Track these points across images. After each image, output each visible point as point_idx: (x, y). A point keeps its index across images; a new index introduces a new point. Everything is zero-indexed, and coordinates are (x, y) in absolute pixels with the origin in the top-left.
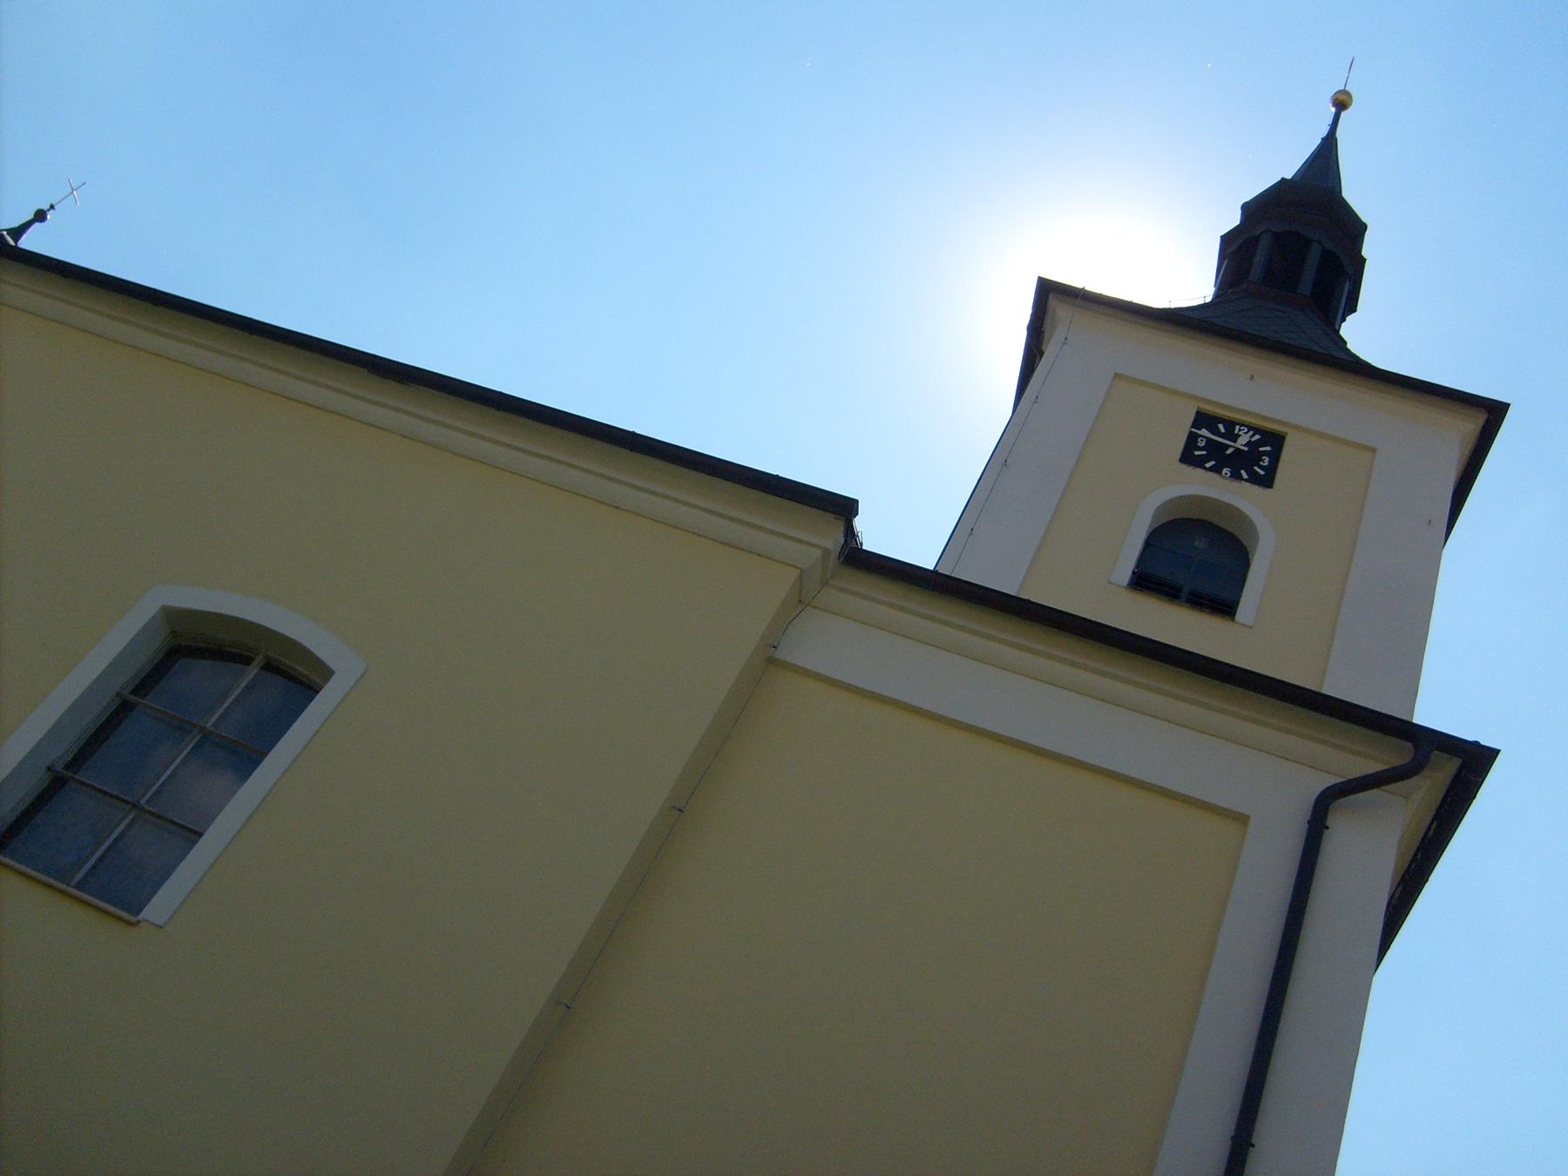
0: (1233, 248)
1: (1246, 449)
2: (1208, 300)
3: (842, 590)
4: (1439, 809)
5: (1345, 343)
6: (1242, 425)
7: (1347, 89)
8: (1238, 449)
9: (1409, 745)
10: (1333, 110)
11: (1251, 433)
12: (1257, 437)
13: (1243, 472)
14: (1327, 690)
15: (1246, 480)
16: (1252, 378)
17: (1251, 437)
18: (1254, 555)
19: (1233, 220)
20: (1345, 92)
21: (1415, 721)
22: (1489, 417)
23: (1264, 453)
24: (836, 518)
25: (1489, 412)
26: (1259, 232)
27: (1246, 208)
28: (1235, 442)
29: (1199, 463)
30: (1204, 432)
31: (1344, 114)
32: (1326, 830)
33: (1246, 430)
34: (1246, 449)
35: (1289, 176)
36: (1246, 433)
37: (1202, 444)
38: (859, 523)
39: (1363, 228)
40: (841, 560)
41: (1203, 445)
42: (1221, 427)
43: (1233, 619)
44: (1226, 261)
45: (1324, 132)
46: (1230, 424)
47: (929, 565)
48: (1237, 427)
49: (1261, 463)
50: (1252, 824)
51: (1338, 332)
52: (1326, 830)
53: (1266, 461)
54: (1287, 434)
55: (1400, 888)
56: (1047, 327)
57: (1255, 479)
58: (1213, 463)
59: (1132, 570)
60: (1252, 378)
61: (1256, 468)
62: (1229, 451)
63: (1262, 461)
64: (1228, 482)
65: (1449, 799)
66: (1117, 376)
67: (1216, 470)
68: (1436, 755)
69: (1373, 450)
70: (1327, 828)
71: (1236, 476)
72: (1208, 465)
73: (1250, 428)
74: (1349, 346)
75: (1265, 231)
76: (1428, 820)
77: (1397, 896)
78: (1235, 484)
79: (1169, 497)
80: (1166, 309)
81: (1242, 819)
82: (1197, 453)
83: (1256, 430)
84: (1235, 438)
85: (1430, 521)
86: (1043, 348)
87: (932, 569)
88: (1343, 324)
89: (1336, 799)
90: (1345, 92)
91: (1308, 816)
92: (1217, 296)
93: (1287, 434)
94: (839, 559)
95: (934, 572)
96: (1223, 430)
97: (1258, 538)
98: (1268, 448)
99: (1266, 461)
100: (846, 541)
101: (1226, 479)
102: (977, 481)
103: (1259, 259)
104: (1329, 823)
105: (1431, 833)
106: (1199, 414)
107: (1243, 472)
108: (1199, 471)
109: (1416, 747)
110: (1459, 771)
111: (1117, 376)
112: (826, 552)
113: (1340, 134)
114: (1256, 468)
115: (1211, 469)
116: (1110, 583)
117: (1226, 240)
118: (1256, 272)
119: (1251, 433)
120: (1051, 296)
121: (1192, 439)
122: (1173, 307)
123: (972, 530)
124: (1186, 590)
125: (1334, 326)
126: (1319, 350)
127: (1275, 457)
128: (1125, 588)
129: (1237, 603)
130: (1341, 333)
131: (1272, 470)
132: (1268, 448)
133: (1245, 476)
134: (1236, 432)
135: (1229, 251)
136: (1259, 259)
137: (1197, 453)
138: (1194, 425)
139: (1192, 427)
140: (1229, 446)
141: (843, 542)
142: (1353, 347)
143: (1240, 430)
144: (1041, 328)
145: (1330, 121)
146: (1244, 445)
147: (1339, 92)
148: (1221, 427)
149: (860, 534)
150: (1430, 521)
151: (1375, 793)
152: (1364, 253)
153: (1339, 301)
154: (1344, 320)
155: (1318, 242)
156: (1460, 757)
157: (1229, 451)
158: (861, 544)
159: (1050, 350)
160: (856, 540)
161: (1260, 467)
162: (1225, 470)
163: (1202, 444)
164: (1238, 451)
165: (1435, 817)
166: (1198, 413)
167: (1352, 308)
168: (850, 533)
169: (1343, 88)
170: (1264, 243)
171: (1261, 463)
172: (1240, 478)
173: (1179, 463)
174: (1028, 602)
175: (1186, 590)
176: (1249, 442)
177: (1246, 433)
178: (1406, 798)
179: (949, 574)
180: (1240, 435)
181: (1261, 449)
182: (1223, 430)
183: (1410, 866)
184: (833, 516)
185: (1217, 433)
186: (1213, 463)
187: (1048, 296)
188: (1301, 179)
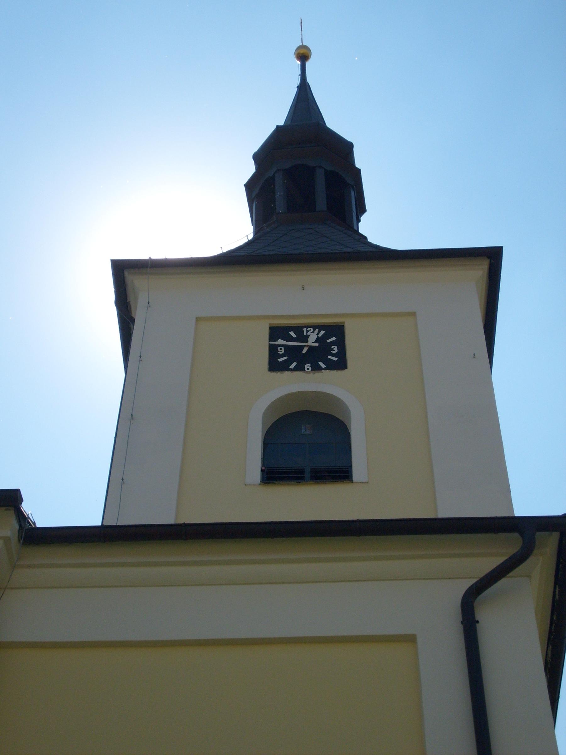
0: (256, 191)
1: (317, 344)
2: (251, 237)
3: (30, 567)
4: (556, 576)
5: (365, 238)
6: (307, 327)
7: (303, 44)
8: (310, 346)
9: (516, 535)
10: (299, 63)
11: (317, 330)
12: (322, 332)
13: (320, 363)
14: (442, 514)
15: (325, 369)
16: (303, 287)
17: (318, 334)
18: (350, 429)
19: (250, 169)
20: (303, 47)
21: (517, 514)
22: (490, 261)
23: (333, 343)
24: (6, 510)
25: (489, 257)
26: (273, 173)
27: (257, 157)
28: (307, 342)
29: (284, 367)
30: (280, 342)
31: (308, 64)
32: (477, 624)
33: (312, 330)
34: (317, 344)
35: (281, 123)
36: (313, 332)
37: (281, 351)
38: (27, 507)
39: (349, 146)
40: (21, 542)
41: (283, 352)
42: (292, 333)
43: (352, 481)
44: (254, 204)
45: (297, 81)
46: (298, 329)
47: (98, 522)
48: (305, 330)
49: (332, 352)
50: (419, 640)
51: (357, 231)
52: (477, 624)
53: (335, 349)
54: (344, 322)
55: (550, 647)
56: (131, 299)
57: (332, 366)
58: (295, 364)
59: (260, 470)
60: (303, 287)
61: (329, 357)
62: (305, 351)
63: (333, 349)
64: (311, 375)
65: (555, 604)
66: (198, 319)
67: (300, 368)
68: (539, 535)
69: (413, 314)
70: (478, 622)
71: (316, 368)
72: (292, 367)
73: (315, 327)
74: (369, 240)
75: (276, 172)
76: (551, 589)
77: (550, 656)
78: (318, 375)
79: (269, 402)
80: (220, 254)
81: (411, 639)
82: (280, 360)
83: (319, 327)
84: (305, 339)
85: (474, 354)
86: (133, 316)
87: (100, 524)
88: (360, 224)
89: (476, 597)
90: (303, 47)
91: (460, 618)
92: (256, 232)
93: (344, 322)
94: (19, 541)
95: (102, 527)
96: (294, 336)
97: (350, 411)
98: (334, 339)
99: (335, 349)
100: (20, 526)
101: (309, 373)
102: (114, 439)
103: (279, 194)
104: (478, 618)
105: (557, 597)
106: (271, 329)
107: (320, 363)
108: (287, 373)
109: (521, 534)
110: (561, 541)
111: (198, 319)
112: (7, 540)
113: (310, 80)
114: (329, 357)
115: (295, 369)
116: (246, 485)
117: (250, 186)
118: (280, 205)
119: (317, 330)
120: (126, 273)
121: (273, 350)
122: (225, 251)
123: (123, 479)
124: (307, 470)
125: (353, 228)
126: (349, 250)
127: (341, 343)
128: (260, 485)
129: (351, 466)
130: (361, 231)
131: (342, 354)
132: (334, 339)
133: (323, 366)
134: (305, 334)
135: (254, 195)
136: (279, 194)
137: (280, 360)
138: (271, 339)
139: (269, 341)
140: (303, 347)
141: (17, 527)
142: (372, 239)
143: (307, 331)
144: (127, 299)
145: (299, 72)
146: (314, 343)
147: (299, 48)
148: (292, 333)
149: (30, 516)
150: (474, 354)
151: (503, 582)
152: (358, 165)
153: (351, 211)
154: (359, 221)
155: (320, 167)
156: (556, 531)
157: (305, 351)
158: (34, 523)
159: (139, 315)
160: (29, 522)
161: (333, 355)
162: (306, 367)
163: (281, 351)
164: (311, 348)
165: (556, 583)
166: (270, 328)
167: (362, 209)
168: (22, 518)
169: (301, 44)
170: (279, 181)
171: (332, 352)
172: (320, 369)
173: (269, 372)
174: (185, 525)
175: (307, 470)
176: (318, 338)
177: (313, 332)
178: (529, 577)
179: (115, 524)
180: (310, 335)
181: (328, 341)
182: (294, 336)
183: (551, 627)
184: (4, 508)
185: (291, 339)
186: (295, 364)
187: (123, 273)
188: (291, 122)
